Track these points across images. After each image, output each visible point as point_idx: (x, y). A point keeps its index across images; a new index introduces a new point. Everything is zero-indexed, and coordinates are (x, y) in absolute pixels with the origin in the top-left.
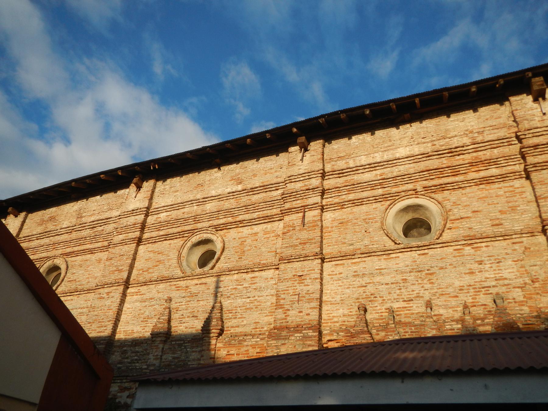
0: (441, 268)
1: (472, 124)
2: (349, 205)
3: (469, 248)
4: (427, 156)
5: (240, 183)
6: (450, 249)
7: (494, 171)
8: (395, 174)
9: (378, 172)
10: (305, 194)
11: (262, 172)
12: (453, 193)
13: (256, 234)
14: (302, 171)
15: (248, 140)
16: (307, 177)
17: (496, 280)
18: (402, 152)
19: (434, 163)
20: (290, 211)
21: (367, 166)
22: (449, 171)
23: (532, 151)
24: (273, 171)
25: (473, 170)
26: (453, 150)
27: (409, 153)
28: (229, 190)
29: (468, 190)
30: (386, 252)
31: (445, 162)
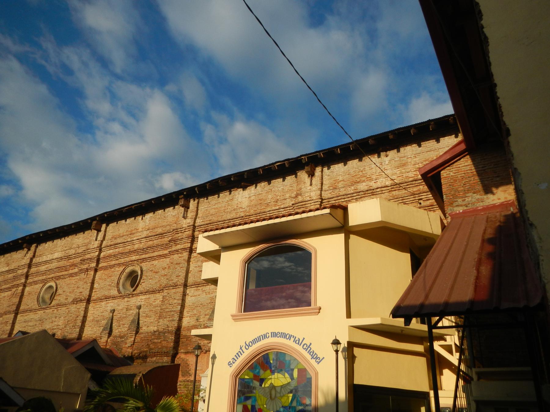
0: (46, 319)
1: (81, 241)
2: (33, 284)
3: (56, 310)
4: (61, 258)
5: (8, 266)
6: (51, 310)
7: (76, 270)
8: (50, 268)
9: (46, 266)
10: (21, 277)
11: (16, 260)
12: (63, 280)
13: (4, 297)
14: (23, 264)
15: (5, 245)
16: (24, 268)
17: (57, 326)
18: (56, 255)
19: (62, 263)
20: (13, 287)
21: (44, 262)
22: (64, 269)
23: (83, 263)
24: (19, 260)
25: (71, 268)
26: (69, 257)
27: (57, 256)
28: (4, 270)
29: (66, 279)
30: (35, 310)
31: (65, 263)
